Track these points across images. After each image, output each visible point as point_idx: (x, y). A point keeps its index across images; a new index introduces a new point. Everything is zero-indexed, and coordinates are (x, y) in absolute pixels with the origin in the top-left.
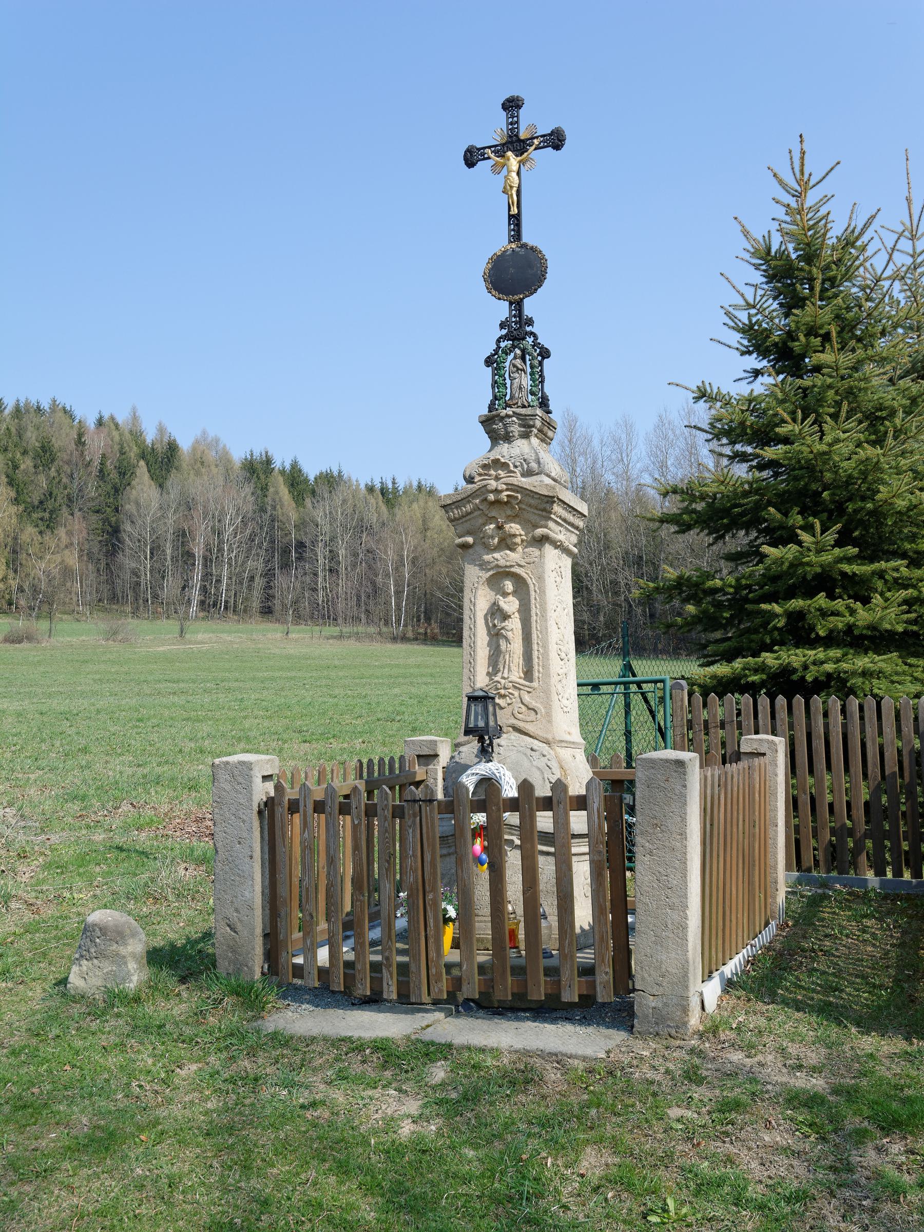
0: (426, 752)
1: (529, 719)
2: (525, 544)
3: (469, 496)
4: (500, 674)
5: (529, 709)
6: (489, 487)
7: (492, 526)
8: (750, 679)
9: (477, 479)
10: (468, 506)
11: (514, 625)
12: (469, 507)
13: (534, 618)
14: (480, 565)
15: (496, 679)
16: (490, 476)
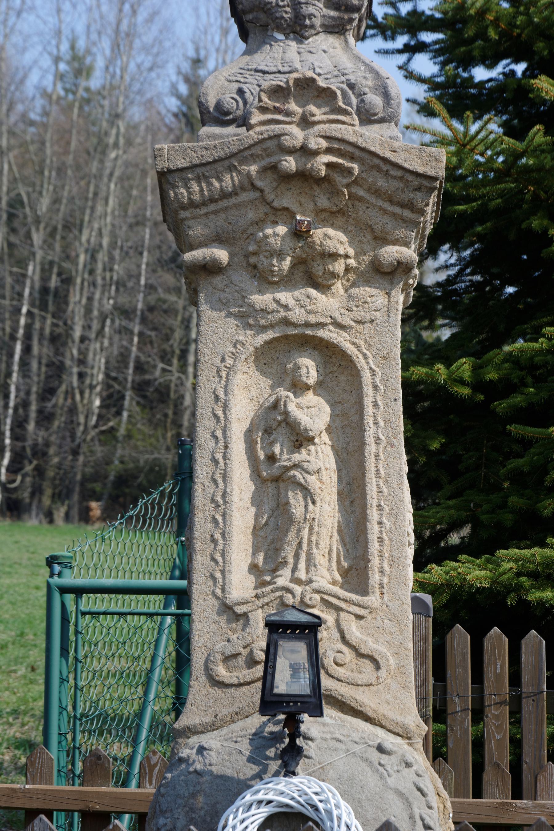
1: (361, 678)
2: (352, 276)
3: (233, 155)
4: (287, 572)
5: (360, 655)
6: (287, 141)
7: (282, 230)
8: (534, 596)
9: (256, 118)
10: (227, 178)
11: (321, 460)
12: (229, 181)
13: (371, 449)
14: (240, 316)
15: (281, 582)
16: (288, 114)
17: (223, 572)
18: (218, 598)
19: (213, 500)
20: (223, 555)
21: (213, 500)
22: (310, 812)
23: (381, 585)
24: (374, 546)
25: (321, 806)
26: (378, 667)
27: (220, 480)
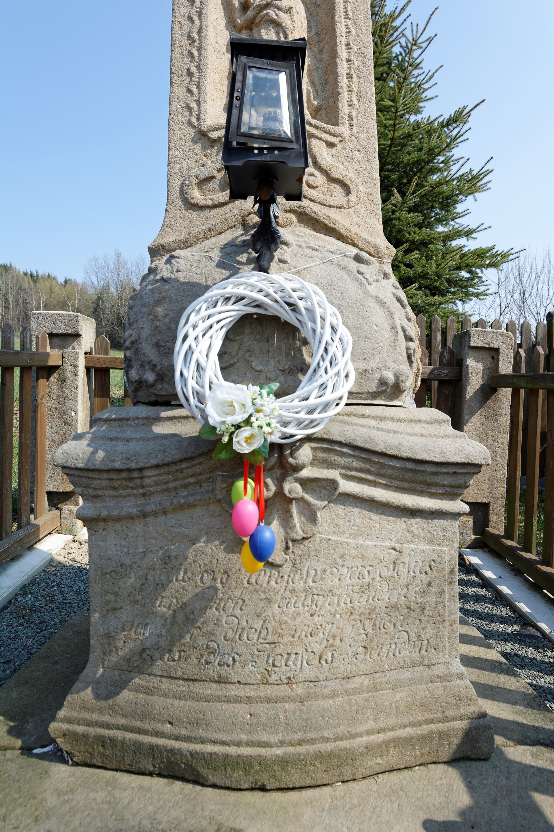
0: (61, 329)
17: (198, 102)
18: (193, 126)
19: (190, 37)
20: (198, 87)
21: (190, 37)
22: (287, 315)
23: (350, 118)
24: (343, 82)
25: (301, 304)
26: (348, 191)
27: (196, 18)
